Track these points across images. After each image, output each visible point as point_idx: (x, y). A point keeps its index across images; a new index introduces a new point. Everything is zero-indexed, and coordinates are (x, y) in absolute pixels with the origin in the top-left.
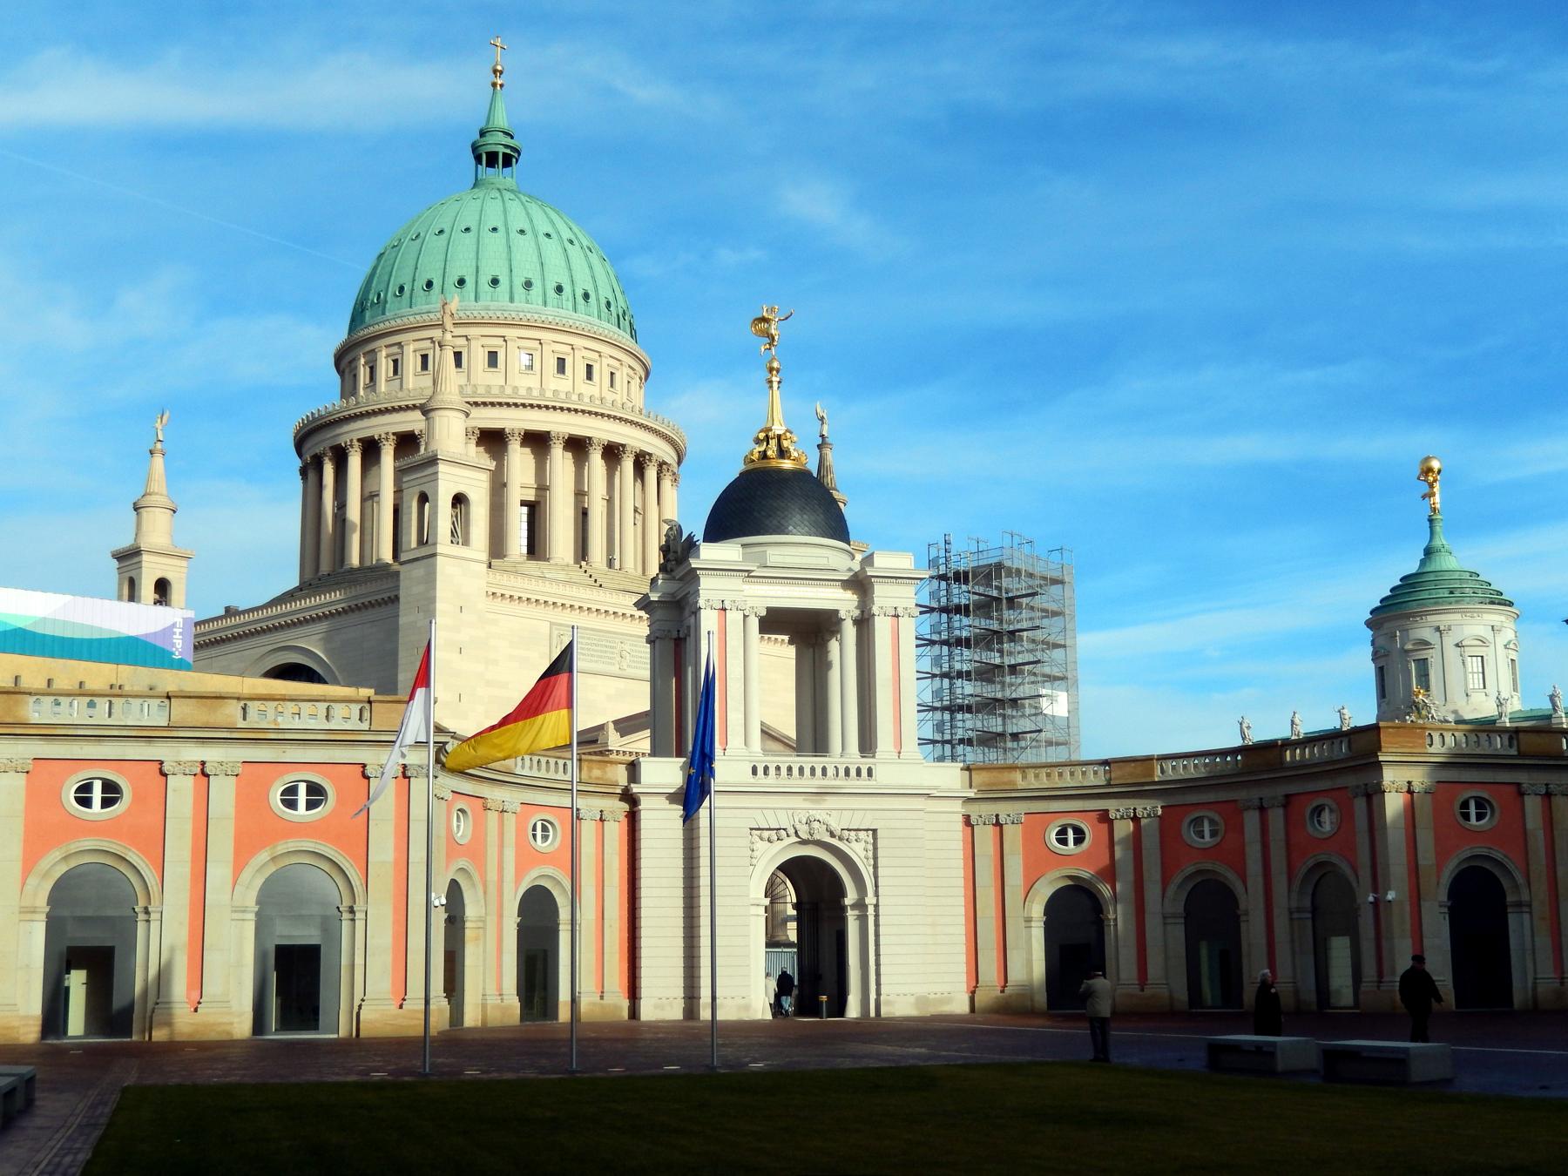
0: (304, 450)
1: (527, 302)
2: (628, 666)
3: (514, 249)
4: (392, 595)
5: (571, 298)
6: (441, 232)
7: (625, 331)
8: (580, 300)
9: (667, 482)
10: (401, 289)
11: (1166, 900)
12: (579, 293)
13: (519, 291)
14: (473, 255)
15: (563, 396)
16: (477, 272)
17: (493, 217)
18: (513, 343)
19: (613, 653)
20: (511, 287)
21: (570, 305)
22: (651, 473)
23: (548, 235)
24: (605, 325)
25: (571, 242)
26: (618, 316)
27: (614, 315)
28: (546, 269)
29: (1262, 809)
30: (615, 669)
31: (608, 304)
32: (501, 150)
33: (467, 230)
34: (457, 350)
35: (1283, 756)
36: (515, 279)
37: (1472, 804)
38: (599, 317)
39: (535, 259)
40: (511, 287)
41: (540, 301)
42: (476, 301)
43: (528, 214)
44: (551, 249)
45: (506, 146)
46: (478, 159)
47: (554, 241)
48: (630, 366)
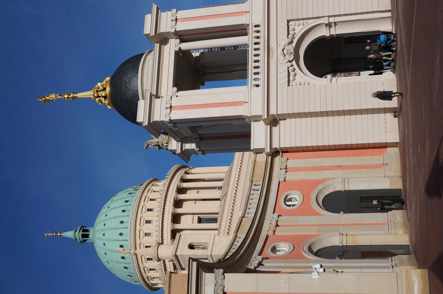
1: (128, 222)
3: (110, 228)
5: (127, 207)
16: (117, 240)
20: (123, 228)
21: (129, 207)
23: (106, 215)
32: (81, 233)
34: (145, 247)
36: (120, 227)
38: (134, 197)
40: (123, 228)
44: (111, 214)
45: (80, 231)
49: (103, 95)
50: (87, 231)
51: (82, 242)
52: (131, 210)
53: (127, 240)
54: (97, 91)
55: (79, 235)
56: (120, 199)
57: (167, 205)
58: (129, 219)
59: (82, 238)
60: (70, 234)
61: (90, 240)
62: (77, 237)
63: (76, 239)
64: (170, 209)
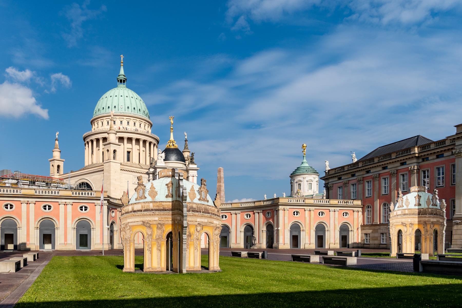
0: (85, 140)
1: (128, 111)
4: (102, 169)
6: (111, 96)
7: (147, 117)
9: (155, 147)
10: (103, 108)
12: (138, 109)
14: (117, 101)
21: (137, 112)
23: (132, 97)
25: (137, 99)
28: (132, 104)
31: (144, 111)
32: (123, 79)
33: (116, 96)
36: (126, 106)
38: (142, 114)
39: (130, 102)
41: (131, 111)
45: (124, 78)
49: (170, 145)
50: (124, 82)
51: (117, 79)
52: (135, 113)
53: (118, 110)
54: (172, 142)
55: (122, 77)
56: (141, 106)
57: (137, 135)
58: (129, 112)
59: (120, 80)
60: (122, 72)
61: (119, 85)
62: (120, 77)
63: (119, 76)
64: (135, 136)
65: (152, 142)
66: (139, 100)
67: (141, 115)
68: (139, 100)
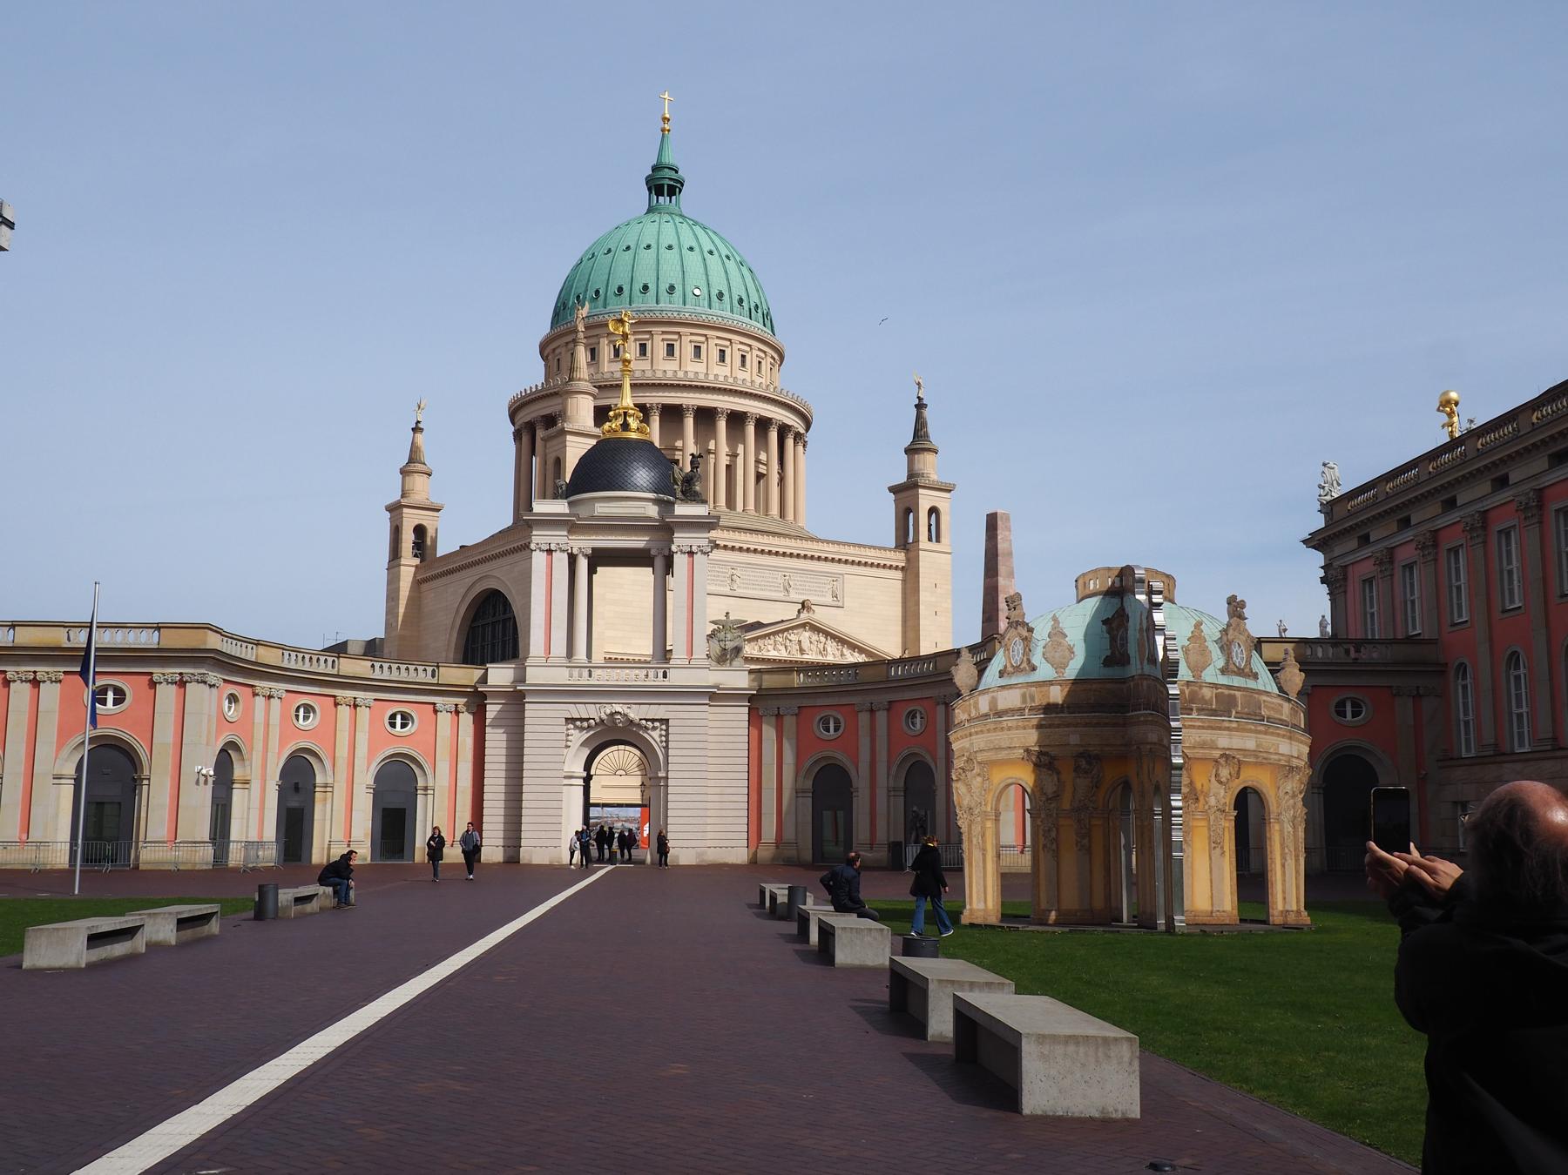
1: (670, 303)
2: (738, 587)
8: (714, 298)
11: (891, 777)
13: (664, 295)
15: (721, 379)
17: (668, 236)
18: (686, 337)
19: (725, 577)
22: (773, 436)
24: (736, 316)
26: (750, 309)
27: (746, 308)
29: (872, 711)
30: (726, 590)
35: (888, 671)
37: (399, 717)
39: (679, 268)
42: (657, 303)
43: (677, 232)
46: (650, 189)
47: (696, 255)
48: (759, 349)
52: (699, 310)
65: (770, 419)
66: (720, 256)
67: (729, 314)
68: (720, 256)
